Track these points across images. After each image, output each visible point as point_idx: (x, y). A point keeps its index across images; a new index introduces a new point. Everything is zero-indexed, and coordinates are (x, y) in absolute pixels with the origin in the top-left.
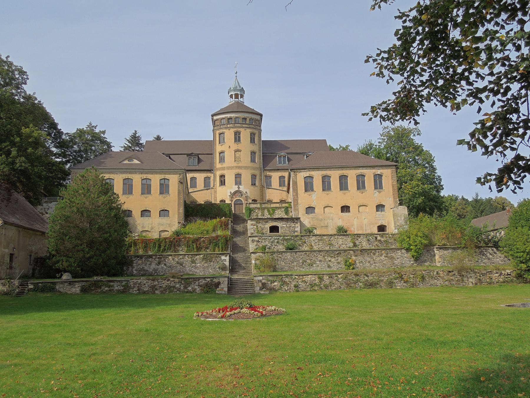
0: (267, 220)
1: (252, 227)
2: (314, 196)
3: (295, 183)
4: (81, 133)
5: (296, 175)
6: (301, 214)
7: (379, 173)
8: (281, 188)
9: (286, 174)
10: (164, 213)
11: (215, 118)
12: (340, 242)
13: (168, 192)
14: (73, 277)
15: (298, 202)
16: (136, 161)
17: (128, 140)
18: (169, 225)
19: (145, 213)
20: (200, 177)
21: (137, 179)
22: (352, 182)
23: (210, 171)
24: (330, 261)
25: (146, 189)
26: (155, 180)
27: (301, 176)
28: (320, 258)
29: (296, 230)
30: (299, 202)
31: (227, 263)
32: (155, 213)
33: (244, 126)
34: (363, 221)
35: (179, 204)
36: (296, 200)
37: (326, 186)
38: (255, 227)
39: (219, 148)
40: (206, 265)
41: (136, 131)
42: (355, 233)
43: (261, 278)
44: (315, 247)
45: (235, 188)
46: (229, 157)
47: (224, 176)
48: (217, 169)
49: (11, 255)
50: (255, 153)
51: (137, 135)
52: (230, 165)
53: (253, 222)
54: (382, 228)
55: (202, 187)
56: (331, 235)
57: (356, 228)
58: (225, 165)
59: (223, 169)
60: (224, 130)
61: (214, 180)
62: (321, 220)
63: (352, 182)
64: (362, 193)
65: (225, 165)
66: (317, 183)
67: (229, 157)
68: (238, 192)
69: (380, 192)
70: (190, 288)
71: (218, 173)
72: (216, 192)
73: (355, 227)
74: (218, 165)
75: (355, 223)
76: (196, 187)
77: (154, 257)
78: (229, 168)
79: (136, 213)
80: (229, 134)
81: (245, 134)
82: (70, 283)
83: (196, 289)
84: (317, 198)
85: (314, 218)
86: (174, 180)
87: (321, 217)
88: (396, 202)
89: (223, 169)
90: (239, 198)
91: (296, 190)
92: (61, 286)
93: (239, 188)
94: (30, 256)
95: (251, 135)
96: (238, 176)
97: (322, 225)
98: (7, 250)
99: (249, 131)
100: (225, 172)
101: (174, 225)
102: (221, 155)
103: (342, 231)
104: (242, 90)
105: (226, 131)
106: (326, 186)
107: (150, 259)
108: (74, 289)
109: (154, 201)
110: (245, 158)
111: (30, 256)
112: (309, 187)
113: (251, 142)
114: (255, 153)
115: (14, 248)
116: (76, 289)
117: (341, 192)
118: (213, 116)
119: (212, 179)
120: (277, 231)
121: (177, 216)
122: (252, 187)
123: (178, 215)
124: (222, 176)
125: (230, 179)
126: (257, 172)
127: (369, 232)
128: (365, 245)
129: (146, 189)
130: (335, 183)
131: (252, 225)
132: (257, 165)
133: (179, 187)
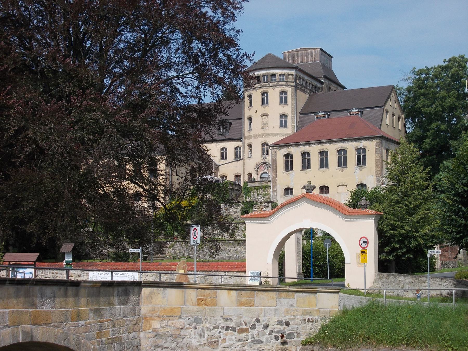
7: (361, 146)
15: (276, 183)
20: (230, 146)
22: (333, 159)
23: (239, 139)
30: (278, 182)
33: (271, 84)
48: (245, 138)
50: (286, 116)
58: (252, 133)
59: (250, 137)
61: (244, 151)
63: (333, 159)
64: (342, 170)
65: (252, 133)
66: (297, 161)
69: (361, 169)
71: (247, 142)
72: (244, 164)
74: (247, 134)
76: (226, 158)
81: (274, 94)
89: (250, 137)
90: (265, 171)
99: (278, 90)
112: (289, 166)
113: (281, 102)
114: (286, 116)
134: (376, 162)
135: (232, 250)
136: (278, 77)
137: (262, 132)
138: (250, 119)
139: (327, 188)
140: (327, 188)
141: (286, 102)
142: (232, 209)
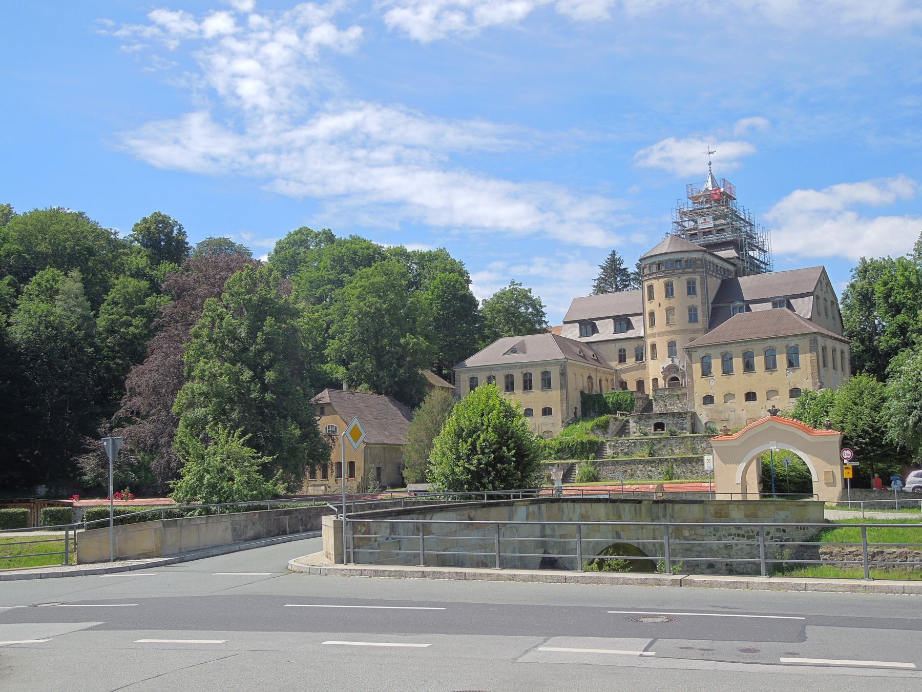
4: (499, 297)
28: (640, 467)
32: (537, 412)
41: (614, 252)
46: (660, 318)
49: (379, 469)
59: (653, 335)
62: (721, 412)
65: (656, 330)
67: (660, 318)
71: (649, 342)
74: (649, 331)
78: (661, 334)
80: (659, 286)
81: (680, 285)
84: (716, 384)
87: (720, 408)
89: (653, 335)
93: (673, 361)
95: (688, 283)
96: (671, 345)
97: (723, 418)
99: (684, 278)
100: (656, 340)
109: (537, 398)
110: (681, 318)
112: (706, 371)
113: (689, 293)
114: (696, 309)
124: (654, 346)
125: (662, 349)
136: (683, 263)
137: (669, 329)
139: (754, 394)
140: (754, 394)
141: (694, 293)
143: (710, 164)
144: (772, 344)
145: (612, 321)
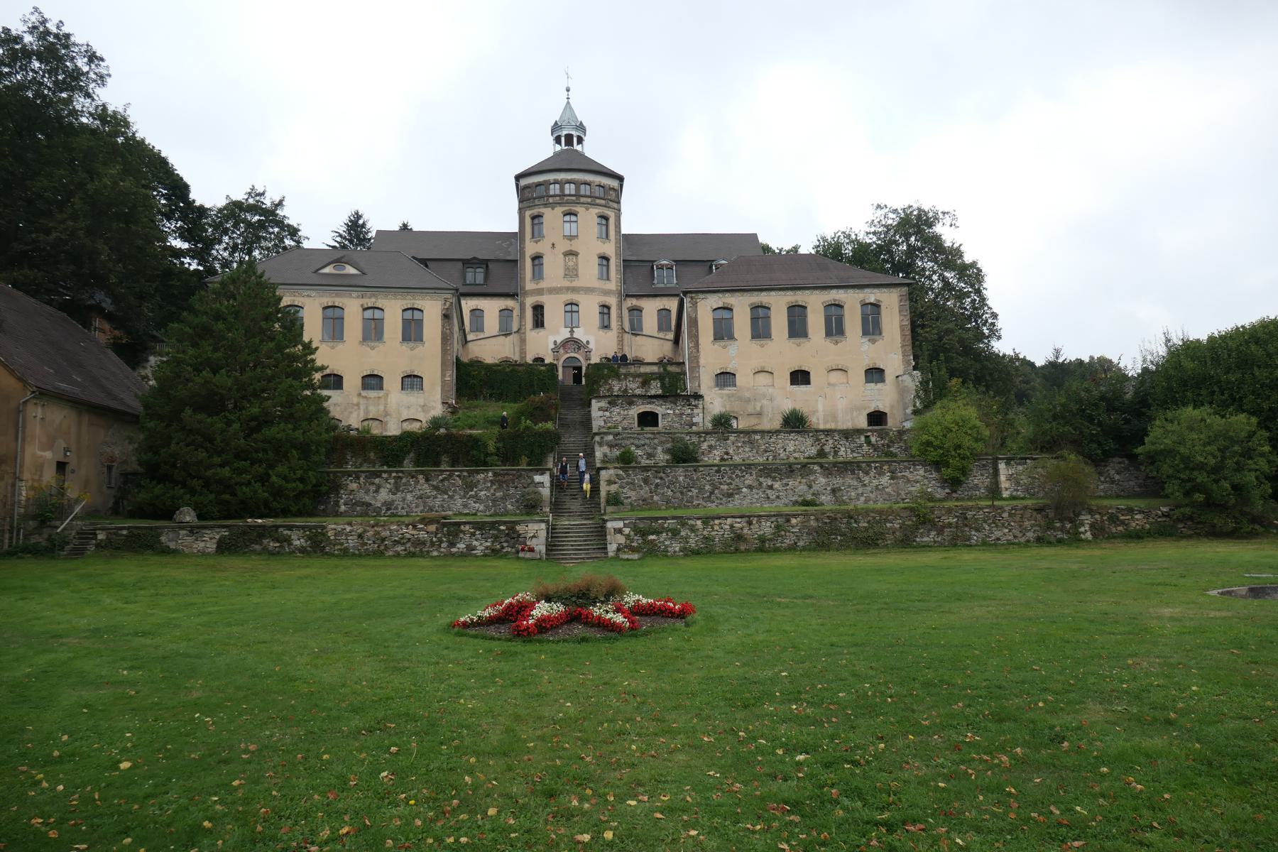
0: (630, 400)
1: (601, 413)
2: (732, 349)
3: (694, 322)
5: (695, 305)
6: (705, 384)
7: (872, 300)
8: (661, 335)
9: (673, 305)
10: (412, 381)
11: (523, 182)
12: (791, 447)
13: (419, 338)
14: (200, 517)
16: (351, 270)
17: (340, 236)
18: (424, 408)
19: (372, 381)
20: (491, 308)
21: (352, 307)
22: (816, 321)
23: (512, 296)
24: (771, 487)
25: (373, 330)
26: (393, 311)
27: (706, 308)
29: (695, 420)
30: (702, 361)
31: (546, 492)
32: (392, 383)
34: (838, 402)
35: (444, 364)
36: (695, 359)
37: (760, 329)
38: (607, 414)
39: (531, 248)
40: (499, 494)
42: (821, 427)
43: (620, 524)
44: (735, 457)
45: (564, 334)
46: (554, 268)
47: (542, 307)
48: (526, 293)
49: (61, 466)
50: (607, 259)
51: (361, 222)
52: (554, 285)
53: (603, 404)
54: (877, 418)
55: (495, 331)
56: (769, 432)
57: (821, 417)
58: (543, 285)
59: (540, 292)
60: (542, 210)
62: (748, 401)
63: (816, 321)
64: (837, 343)
65: (543, 285)
68: (572, 343)
69: (873, 341)
70: (462, 546)
72: (523, 341)
73: (821, 414)
74: (529, 286)
75: (820, 407)
76: (482, 331)
77: (385, 475)
79: (352, 382)
82: (193, 530)
83: (474, 548)
84: (741, 353)
85: (733, 395)
86: (432, 310)
87: (747, 395)
88: (908, 363)
89: (540, 292)
91: (695, 337)
92: (171, 535)
93: (572, 332)
94: (110, 468)
97: (750, 410)
98: (48, 455)
99: (594, 211)
101: (434, 408)
102: (536, 262)
103: (795, 422)
104: (581, 127)
105: (547, 212)
106: (760, 329)
107: (377, 481)
108: (202, 544)
109: (391, 357)
111: (110, 468)
112: (723, 332)
115: (66, 450)
116: (208, 542)
117: (792, 340)
118: (518, 178)
119: (516, 313)
120: (656, 425)
121: (439, 389)
122: (602, 332)
123: (443, 387)
124: (538, 310)
126: (612, 301)
127: (848, 425)
128: (845, 453)
129: (373, 330)
130: (779, 322)
131: (600, 409)
132: (612, 285)
133: (443, 326)
134: (902, 330)
135: (777, 485)
137: (566, 283)
138: (537, 258)
142: (616, 410)
143: (568, 90)
144: (837, 297)
145: (460, 264)
